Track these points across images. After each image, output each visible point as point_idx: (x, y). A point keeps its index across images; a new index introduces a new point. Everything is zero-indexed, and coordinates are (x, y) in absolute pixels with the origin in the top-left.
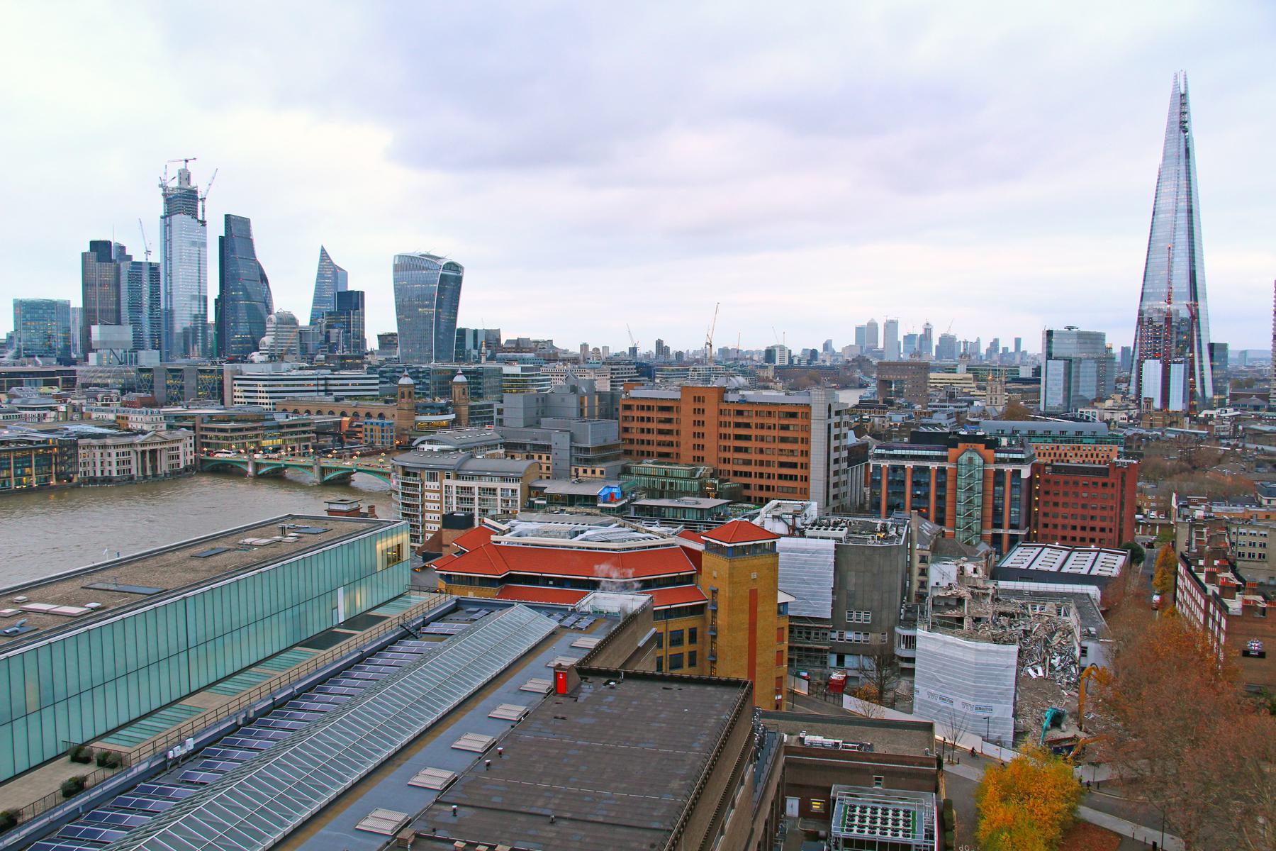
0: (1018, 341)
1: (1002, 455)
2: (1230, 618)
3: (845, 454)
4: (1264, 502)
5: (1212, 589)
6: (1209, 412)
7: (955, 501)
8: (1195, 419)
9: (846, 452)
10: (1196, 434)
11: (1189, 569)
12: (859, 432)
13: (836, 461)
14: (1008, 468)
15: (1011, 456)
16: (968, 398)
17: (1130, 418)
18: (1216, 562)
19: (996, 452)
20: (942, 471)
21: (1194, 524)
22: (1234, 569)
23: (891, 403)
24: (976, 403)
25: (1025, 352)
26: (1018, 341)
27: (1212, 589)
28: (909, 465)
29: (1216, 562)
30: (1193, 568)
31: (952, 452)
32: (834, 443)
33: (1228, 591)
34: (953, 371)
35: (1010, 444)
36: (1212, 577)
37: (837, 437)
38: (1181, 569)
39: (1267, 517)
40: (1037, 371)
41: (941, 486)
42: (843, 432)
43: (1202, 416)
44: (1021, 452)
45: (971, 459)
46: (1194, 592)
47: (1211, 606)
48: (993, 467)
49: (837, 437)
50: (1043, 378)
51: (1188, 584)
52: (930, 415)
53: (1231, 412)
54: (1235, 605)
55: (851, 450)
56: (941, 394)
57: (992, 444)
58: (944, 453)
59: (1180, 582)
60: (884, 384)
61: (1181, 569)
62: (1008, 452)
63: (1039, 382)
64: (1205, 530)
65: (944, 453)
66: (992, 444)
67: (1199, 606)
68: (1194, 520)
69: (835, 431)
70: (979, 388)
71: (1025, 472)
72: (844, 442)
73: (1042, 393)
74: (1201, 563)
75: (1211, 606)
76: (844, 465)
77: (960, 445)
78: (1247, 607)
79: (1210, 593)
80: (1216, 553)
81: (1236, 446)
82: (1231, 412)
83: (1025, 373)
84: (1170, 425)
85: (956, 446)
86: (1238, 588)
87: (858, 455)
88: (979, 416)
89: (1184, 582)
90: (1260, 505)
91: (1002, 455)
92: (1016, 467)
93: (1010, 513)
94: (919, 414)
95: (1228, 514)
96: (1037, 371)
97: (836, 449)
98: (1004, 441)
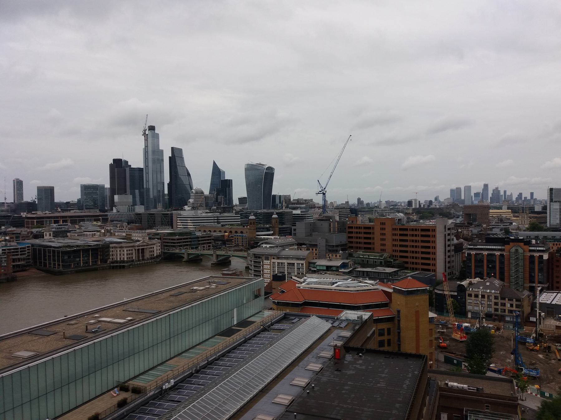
1: (533, 248)
3: (453, 248)
7: (510, 270)
9: (454, 247)
12: (458, 236)
14: (537, 254)
15: (538, 248)
19: (530, 247)
20: (502, 255)
23: (471, 224)
24: (514, 224)
25: (536, 199)
31: (507, 247)
32: (448, 243)
34: (500, 208)
35: (537, 243)
37: (449, 240)
40: (545, 208)
41: (502, 263)
42: (452, 238)
44: (543, 247)
45: (517, 250)
48: (529, 254)
49: (449, 240)
52: (491, 229)
57: (527, 243)
58: (503, 247)
60: (468, 215)
62: (536, 247)
63: (546, 213)
65: (503, 247)
69: (448, 237)
70: (514, 216)
71: (546, 257)
72: (452, 242)
73: (548, 218)
77: (511, 243)
83: (538, 208)
85: (509, 244)
87: (458, 248)
91: (533, 248)
92: (541, 254)
93: (538, 276)
94: (486, 229)
96: (545, 208)
97: (449, 246)
98: (534, 242)
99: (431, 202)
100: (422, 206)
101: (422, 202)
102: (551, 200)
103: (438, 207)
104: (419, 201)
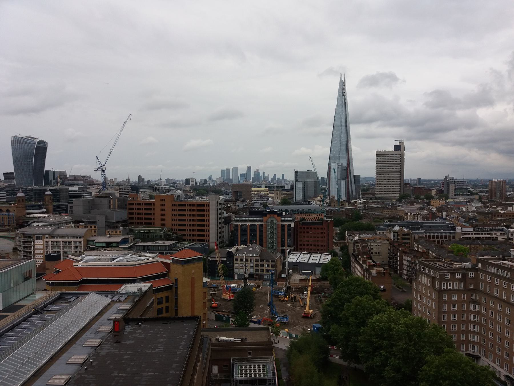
0: (283, 175)
2: (373, 277)
3: (223, 220)
4: (378, 233)
5: (365, 266)
6: (355, 201)
7: (267, 237)
8: (351, 203)
10: (351, 209)
11: (356, 259)
13: (220, 223)
14: (286, 224)
15: (287, 219)
16: (267, 197)
17: (327, 203)
18: (365, 256)
21: (355, 242)
22: (371, 259)
23: (238, 200)
26: (283, 175)
27: (365, 266)
28: (249, 223)
29: (365, 256)
30: (357, 259)
31: (265, 218)
32: (219, 216)
33: (371, 267)
35: (286, 214)
36: (364, 262)
37: (220, 214)
38: (353, 259)
39: (380, 239)
40: (292, 187)
43: (352, 202)
45: (272, 221)
46: (359, 268)
47: (365, 273)
48: (281, 223)
49: (220, 214)
50: (294, 189)
51: (356, 265)
53: (362, 200)
54: (374, 272)
55: (226, 218)
56: (257, 196)
57: (280, 214)
58: (262, 219)
59: (352, 264)
61: (353, 259)
62: (286, 217)
63: (293, 190)
64: (359, 244)
65: (262, 219)
66: (280, 214)
67: (361, 273)
68: (355, 241)
69: (219, 211)
70: (270, 193)
71: (292, 225)
73: (294, 195)
74: (360, 257)
75: (365, 273)
76: (223, 225)
77: (268, 215)
78: (379, 273)
79: (364, 268)
80: (365, 253)
81: (366, 213)
82: (362, 200)
83: (287, 187)
84: (341, 206)
86: (374, 266)
88: (272, 204)
89: (354, 264)
90: (377, 234)
91: (284, 219)
92: (289, 223)
94: (249, 204)
95: (366, 238)
96: (292, 187)
98: (284, 213)
99: (205, 181)
100: (198, 184)
101: (198, 180)
102: (297, 181)
103: (211, 185)
104: (196, 180)
